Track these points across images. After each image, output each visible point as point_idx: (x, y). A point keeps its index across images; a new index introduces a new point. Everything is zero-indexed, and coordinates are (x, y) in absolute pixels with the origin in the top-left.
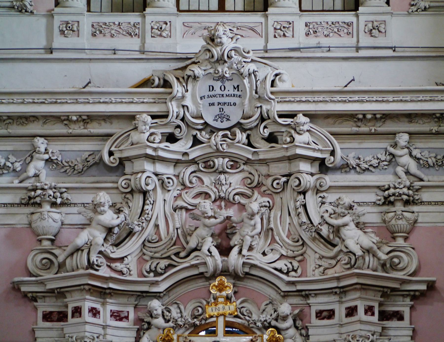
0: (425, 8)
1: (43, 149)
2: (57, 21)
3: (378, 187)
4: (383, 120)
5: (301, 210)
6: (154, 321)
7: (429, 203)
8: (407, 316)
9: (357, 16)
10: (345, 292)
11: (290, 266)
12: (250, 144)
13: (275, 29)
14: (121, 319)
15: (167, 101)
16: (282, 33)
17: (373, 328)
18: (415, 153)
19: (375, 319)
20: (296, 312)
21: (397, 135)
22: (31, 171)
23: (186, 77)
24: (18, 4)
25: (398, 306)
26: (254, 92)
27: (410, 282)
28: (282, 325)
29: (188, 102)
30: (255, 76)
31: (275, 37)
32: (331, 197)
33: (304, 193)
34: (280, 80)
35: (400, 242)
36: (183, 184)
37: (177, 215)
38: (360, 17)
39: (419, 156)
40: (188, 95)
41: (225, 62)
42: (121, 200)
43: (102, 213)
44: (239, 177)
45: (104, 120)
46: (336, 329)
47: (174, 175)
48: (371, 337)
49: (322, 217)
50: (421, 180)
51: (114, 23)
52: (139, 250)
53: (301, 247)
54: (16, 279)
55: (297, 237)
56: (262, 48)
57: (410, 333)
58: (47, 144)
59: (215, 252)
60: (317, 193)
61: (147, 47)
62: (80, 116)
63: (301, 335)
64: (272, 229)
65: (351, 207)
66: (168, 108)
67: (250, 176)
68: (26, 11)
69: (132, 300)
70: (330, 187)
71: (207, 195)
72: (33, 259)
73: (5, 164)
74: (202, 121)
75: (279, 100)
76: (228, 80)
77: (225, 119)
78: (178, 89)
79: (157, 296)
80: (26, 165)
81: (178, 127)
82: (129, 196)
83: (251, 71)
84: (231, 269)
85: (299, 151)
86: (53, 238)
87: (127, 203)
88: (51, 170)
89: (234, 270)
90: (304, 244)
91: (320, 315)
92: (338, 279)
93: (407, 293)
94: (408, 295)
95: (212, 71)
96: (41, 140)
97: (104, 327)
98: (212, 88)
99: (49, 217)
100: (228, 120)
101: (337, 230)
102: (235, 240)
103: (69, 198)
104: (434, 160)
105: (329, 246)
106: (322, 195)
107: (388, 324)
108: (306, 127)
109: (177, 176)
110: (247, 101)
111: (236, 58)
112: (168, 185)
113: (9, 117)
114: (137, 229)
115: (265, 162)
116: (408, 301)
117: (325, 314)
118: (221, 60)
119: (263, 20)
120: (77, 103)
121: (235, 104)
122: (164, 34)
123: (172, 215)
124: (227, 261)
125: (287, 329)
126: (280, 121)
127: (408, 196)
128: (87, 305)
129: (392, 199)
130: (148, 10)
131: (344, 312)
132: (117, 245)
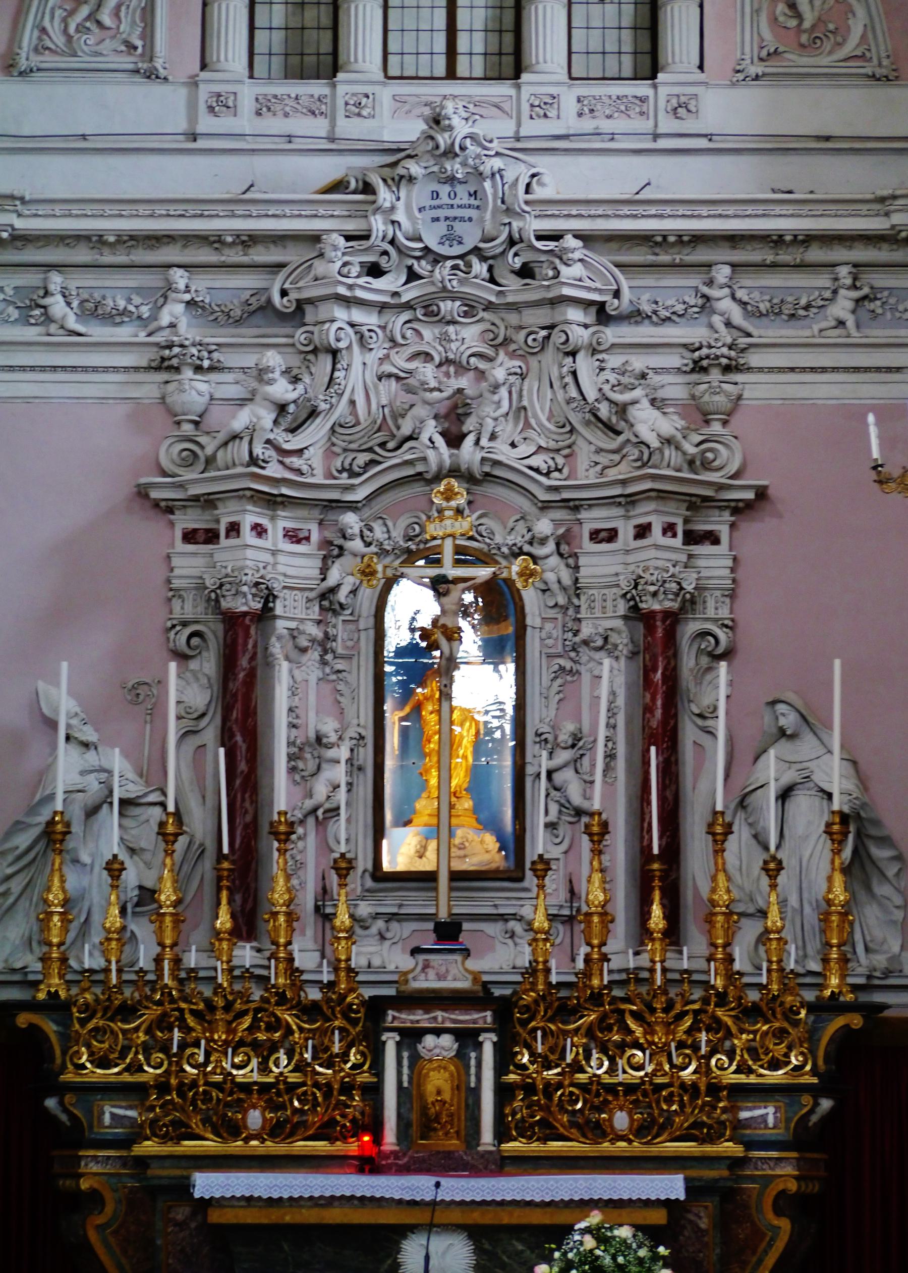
0: (757, 76)
1: (182, 286)
2: (204, 92)
3: (685, 346)
4: (692, 245)
5: (569, 379)
6: (349, 545)
7: (761, 370)
8: (725, 538)
9: (655, 87)
10: (633, 503)
11: (551, 463)
12: (492, 280)
13: (532, 106)
14: (299, 541)
15: (369, 213)
16: (542, 112)
17: (674, 556)
18: (740, 294)
19: (678, 542)
20: (561, 531)
21: (714, 268)
22: (165, 319)
23: (397, 178)
26: (499, 201)
27: (730, 487)
28: (540, 551)
30: (502, 177)
31: (531, 118)
32: (614, 361)
33: (573, 354)
34: (539, 183)
35: (716, 428)
36: (392, 340)
37: (383, 386)
39: (745, 299)
40: (400, 205)
41: (457, 155)
42: (298, 364)
43: (270, 382)
44: (476, 329)
45: (274, 242)
46: (620, 558)
47: (379, 327)
48: (672, 570)
49: (600, 390)
50: (749, 335)
51: (289, 96)
52: (326, 438)
53: (568, 436)
54: (143, 480)
55: (562, 420)
56: (512, 135)
57: (730, 563)
58: (189, 279)
59: (440, 441)
60: (593, 355)
61: (339, 133)
62: (238, 236)
63: (568, 566)
64: (525, 408)
65: (643, 376)
66: (370, 225)
67: (493, 328)
68: (157, 77)
69: (316, 513)
70: (613, 345)
71: (428, 357)
72: (167, 450)
73: (125, 308)
74: (421, 245)
75: (538, 213)
76: (461, 183)
77: (455, 242)
78: (384, 195)
79: (352, 506)
80: (157, 309)
81: (385, 253)
82: (311, 357)
83: (496, 169)
84: (464, 467)
85: (567, 291)
86: (197, 419)
87: (308, 367)
88: (195, 317)
89: (468, 469)
90: (572, 431)
91: (595, 536)
92: (624, 482)
94: (727, 507)
96: (180, 272)
97: (274, 553)
98: (436, 195)
99: (192, 388)
100: (460, 243)
101: (622, 409)
102: (470, 424)
103: (222, 359)
105: (611, 434)
106: (600, 357)
107: (696, 549)
108: (577, 255)
109: (383, 328)
110: (488, 216)
111: (473, 149)
112: (370, 341)
113: (132, 238)
114: (323, 406)
115: (514, 307)
116: (727, 516)
117: (603, 535)
118: (449, 153)
119: (512, 92)
120: (234, 216)
121: (470, 219)
122: (365, 113)
123: (376, 387)
124: (457, 456)
125: (547, 557)
126: (539, 245)
127: (729, 359)
128: (248, 520)
129: (705, 363)
130: (341, 76)
131: (631, 532)
132: (293, 430)
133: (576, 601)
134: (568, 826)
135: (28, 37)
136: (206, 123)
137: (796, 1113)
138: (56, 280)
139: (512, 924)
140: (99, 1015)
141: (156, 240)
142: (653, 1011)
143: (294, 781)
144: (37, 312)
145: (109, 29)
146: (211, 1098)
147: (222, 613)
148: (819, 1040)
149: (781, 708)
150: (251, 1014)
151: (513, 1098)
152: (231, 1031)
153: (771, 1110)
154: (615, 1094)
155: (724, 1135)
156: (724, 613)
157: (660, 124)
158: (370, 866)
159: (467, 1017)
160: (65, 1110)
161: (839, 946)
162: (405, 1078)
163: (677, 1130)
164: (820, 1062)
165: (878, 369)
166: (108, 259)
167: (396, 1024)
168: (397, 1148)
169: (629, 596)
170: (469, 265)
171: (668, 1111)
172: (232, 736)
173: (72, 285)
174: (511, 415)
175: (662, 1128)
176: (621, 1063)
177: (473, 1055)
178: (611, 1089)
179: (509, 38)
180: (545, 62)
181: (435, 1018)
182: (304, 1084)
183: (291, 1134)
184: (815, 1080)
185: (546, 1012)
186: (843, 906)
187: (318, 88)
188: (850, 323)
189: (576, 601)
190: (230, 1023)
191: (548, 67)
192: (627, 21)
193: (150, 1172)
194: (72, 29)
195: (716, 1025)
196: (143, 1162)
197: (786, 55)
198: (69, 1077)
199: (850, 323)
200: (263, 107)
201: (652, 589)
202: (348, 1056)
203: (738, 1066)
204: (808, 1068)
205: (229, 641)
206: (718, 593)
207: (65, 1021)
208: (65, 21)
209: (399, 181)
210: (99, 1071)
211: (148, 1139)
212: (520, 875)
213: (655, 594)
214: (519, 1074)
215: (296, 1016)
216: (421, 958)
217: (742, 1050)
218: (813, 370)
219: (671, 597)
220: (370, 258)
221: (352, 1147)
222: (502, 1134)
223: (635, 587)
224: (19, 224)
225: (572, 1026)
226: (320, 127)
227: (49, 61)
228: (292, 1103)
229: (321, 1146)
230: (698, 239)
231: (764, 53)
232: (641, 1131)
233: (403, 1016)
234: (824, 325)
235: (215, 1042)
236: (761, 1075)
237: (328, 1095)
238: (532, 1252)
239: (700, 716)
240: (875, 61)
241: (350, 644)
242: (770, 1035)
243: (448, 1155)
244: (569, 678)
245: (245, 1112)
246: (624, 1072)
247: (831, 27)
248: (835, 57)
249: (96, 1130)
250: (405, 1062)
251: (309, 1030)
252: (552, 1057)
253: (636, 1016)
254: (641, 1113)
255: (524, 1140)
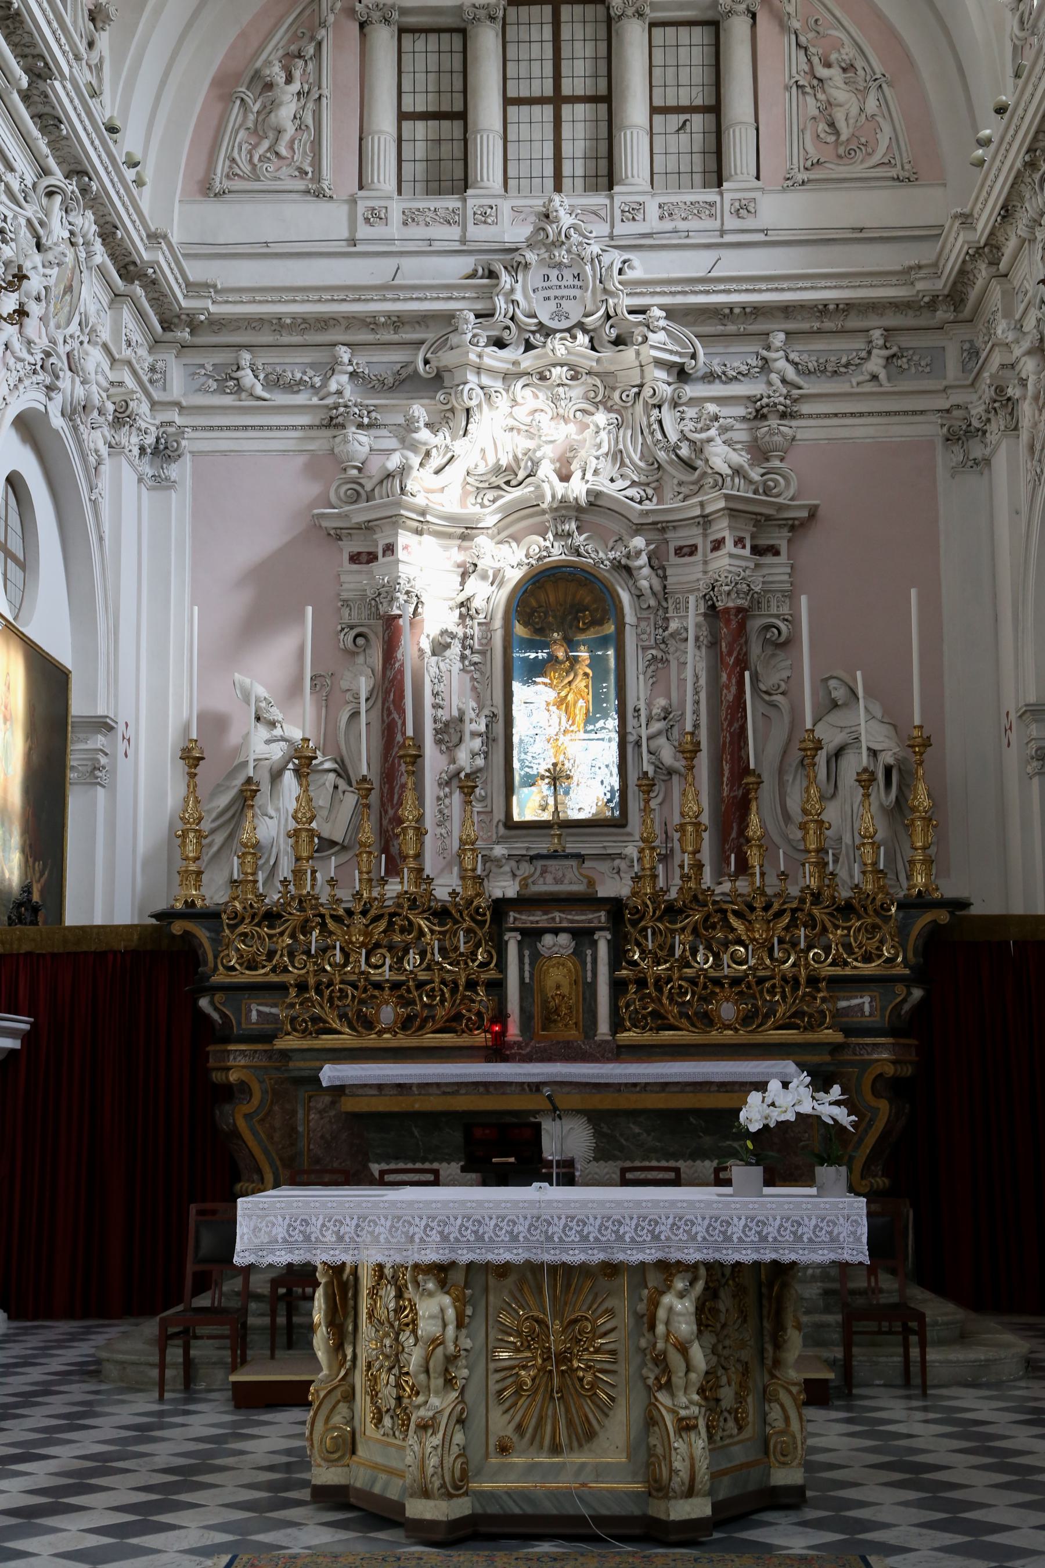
0: (803, 182)
1: (346, 361)
2: (361, 207)
3: (749, 398)
5: (656, 426)
7: (810, 416)
8: (784, 550)
9: (721, 194)
11: (642, 493)
12: (593, 349)
13: (623, 211)
16: (631, 217)
17: (744, 564)
18: (792, 356)
19: (747, 552)
20: (652, 547)
22: (333, 387)
23: (515, 265)
24: (314, 187)
25: (773, 538)
27: (788, 507)
29: (518, 296)
31: (622, 221)
32: (691, 412)
33: (660, 407)
34: (629, 267)
35: (776, 463)
38: (725, 195)
39: (797, 360)
40: (518, 287)
41: (563, 243)
42: (439, 420)
43: (416, 430)
48: (742, 573)
49: (682, 431)
50: (800, 388)
51: (429, 209)
54: (316, 511)
57: (789, 570)
61: (469, 236)
65: (716, 418)
67: (594, 388)
70: (691, 399)
72: (337, 490)
74: (535, 321)
75: (629, 291)
78: (505, 279)
80: (326, 380)
81: (508, 328)
83: (595, 254)
90: (660, 467)
91: (679, 551)
93: (784, 522)
95: (546, 255)
96: (344, 348)
98: (546, 278)
99: (353, 440)
101: (698, 448)
102: (575, 466)
104: (816, 364)
106: (681, 409)
108: (662, 323)
111: (575, 237)
116: (786, 533)
117: (685, 550)
119: (607, 202)
121: (575, 298)
122: (489, 221)
125: (641, 568)
126: (631, 317)
129: (765, 410)
130: (470, 192)
131: (709, 546)
133: (664, 604)
134: (662, 783)
135: (221, 166)
136: (363, 231)
137: (891, 1002)
138: (246, 357)
139: (617, 862)
140: (247, 921)
141: (325, 323)
142: (752, 909)
143: (441, 750)
144: (231, 383)
145: (284, 158)
146: (347, 996)
147: (380, 617)
148: (908, 935)
149: (832, 683)
150: (387, 917)
151: (627, 991)
152: (367, 934)
153: (867, 1000)
154: (721, 985)
155: (824, 1023)
156: (785, 610)
157: (725, 223)
158: (502, 817)
159: (583, 917)
160: (216, 1009)
161: (924, 848)
162: (527, 975)
163: (778, 1020)
164: (910, 954)
165: (906, 413)
166: (286, 339)
167: (519, 925)
168: (520, 1039)
169: (707, 597)
170: (574, 337)
171: (770, 1001)
172: (390, 714)
173: (259, 363)
174: (610, 456)
175: (766, 1017)
176: (726, 958)
177: (589, 952)
178: (717, 982)
179: (603, 164)
180: (633, 176)
181: (553, 919)
182: (432, 981)
183: (421, 1028)
184: (907, 971)
185: (654, 912)
186: (926, 812)
187: (451, 202)
188: (882, 376)
189: (664, 604)
190: (367, 926)
191: (636, 180)
192: (697, 147)
193: (291, 1065)
194: (256, 159)
195: (811, 923)
196: (286, 1055)
197: (826, 165)
198: (220, 978)
199: (882, 376)
200: (409, 218)
201: (727, 588)
202: (476, 955)
203: (834, 960)
204: (900, 959)
205: (386, 638)
206: (779, 595)
207: (217, 930)
208: (250, 152)
209: (516, 268)
210: (247, 972)
211: (289, 1034)
212: (624, 822)
213: (729, 594)
214: (631, 970)
215: (427, 919)
216: (540, 863)
217: (837, 945)
218: (853, 415)
219: (741, 596)
220: (495, 333)
221: (480, 1038)
222: (617, 1025)
223: (713, 589)
224: (213, 309)
225: (679, 925)
226: (455, 232)
227: (237, 184)
228: (421, 999)
229: (447, 1039)
230: (757, 311)
231: (809, 163)
232: (746, 1020)
233: (523, 917)
234: (861, 378)
235: (352, 943)
236: (855, 967)
237: (454, 990)
238: (649, 1135)
239: (766, 692)
240: (899, 166)
241: (484, 641)
242: (863, 930)
243: (568, 1044)
244: (660, 665)
245: (379, 1006)
246: (729, 966)
247: (863, 140)
248: (867, 165)
249: (244, 1026)
250: (527, 960)
251: (440, 933)
252: (660, 953)
253: (737, 914)
254: (746, 1004)
255: (637, 1030)
